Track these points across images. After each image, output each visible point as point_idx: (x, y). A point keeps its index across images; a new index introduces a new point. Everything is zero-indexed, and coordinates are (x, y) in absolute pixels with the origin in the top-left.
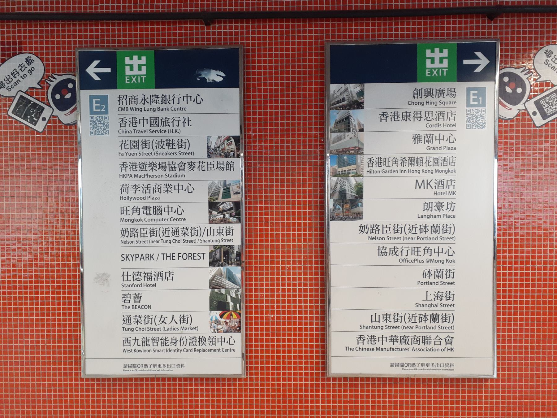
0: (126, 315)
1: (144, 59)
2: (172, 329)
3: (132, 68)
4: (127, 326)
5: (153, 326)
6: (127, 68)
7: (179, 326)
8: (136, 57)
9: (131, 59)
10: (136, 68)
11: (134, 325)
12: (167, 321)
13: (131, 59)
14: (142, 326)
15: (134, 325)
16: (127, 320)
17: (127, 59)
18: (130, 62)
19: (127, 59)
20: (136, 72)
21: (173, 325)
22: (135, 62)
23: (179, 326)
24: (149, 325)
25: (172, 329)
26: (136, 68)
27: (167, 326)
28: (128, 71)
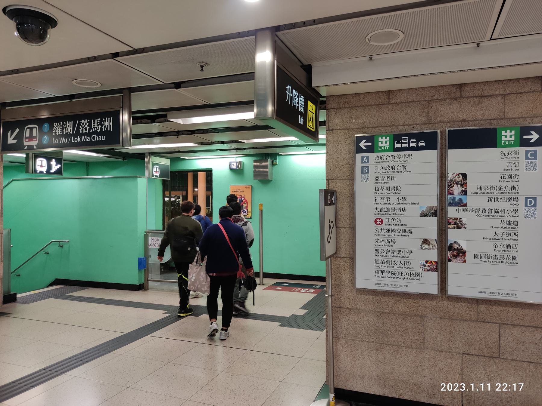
0: (377, 259)
1: (388, 138)
2: (400, 267)
3: (382, 143)
5: (391, 265)
6: (380, 143)
7: (403, 266)
9: (382, 138)
10: (384, 142)
11: (380, 265)
13: (382, 138)
15: (380, 265)
16: (377, 262)
17: (380, 139)
18: (381, 140)
19: (380, 139)
20: (384, 144)
21: (401, 265)
23: (403, 266)
24: (388, 265)
25: (400, 267)
26: (384, 142)
27: (397, 266)
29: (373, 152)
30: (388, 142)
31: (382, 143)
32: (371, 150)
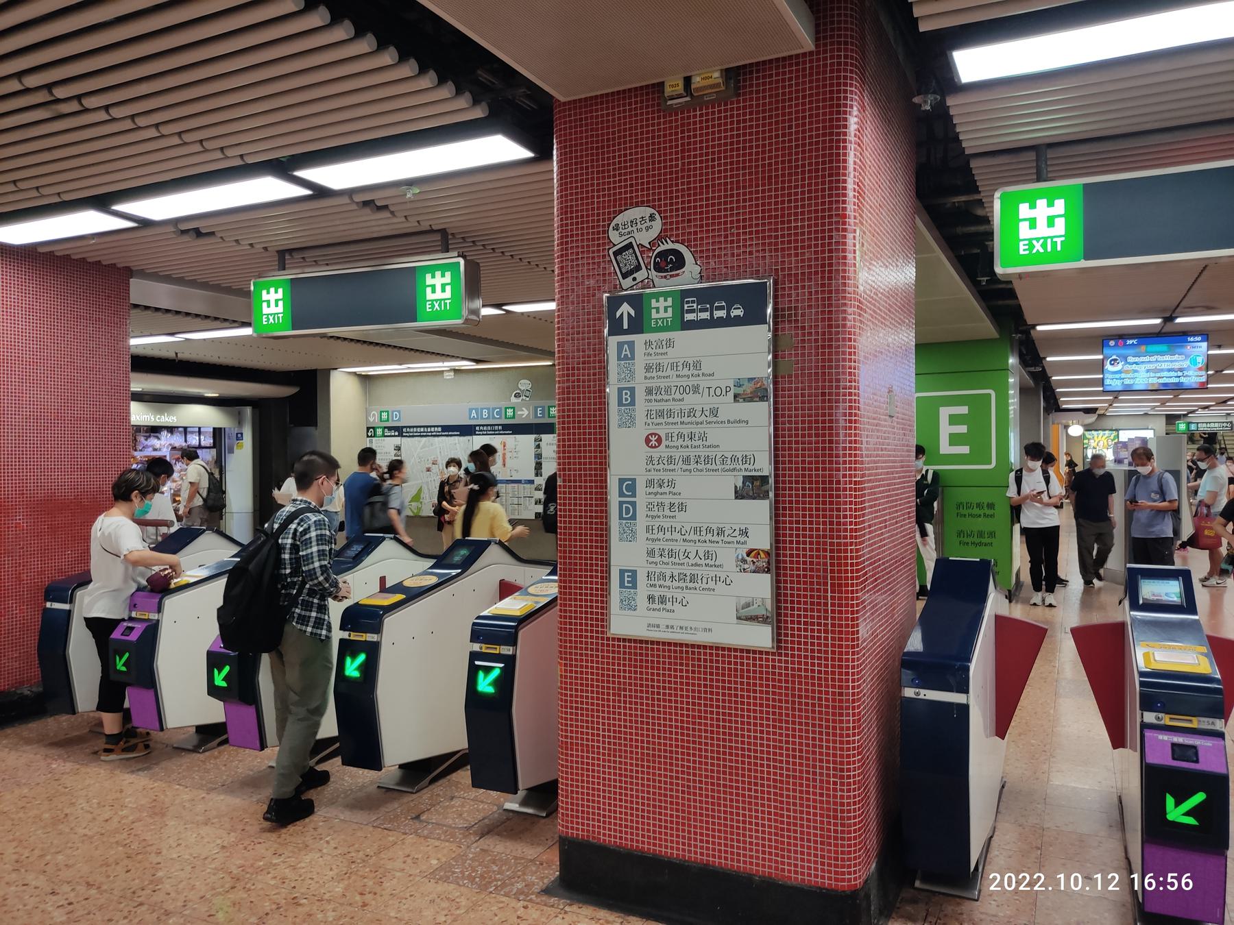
0: (650, 547)
2: (696, 565)
3: (658, 312)
4: (651, 560)
5: (677, 560)
6: (654, 311)
8: (662, 299)
10: (662, 310)
11: (657, 559)
12: (692, 555)
14: (666, 560)
18: (657, 305)
20: (662, 314)
22: (662, 303)
23: (703, 562)
25: (696, 565)
26: (662, 310)
27: (691, 562)
28: (654, 315)
29: (641, 332)
30: (670, 310)
31: (658, 312)
32: (637, 325)
